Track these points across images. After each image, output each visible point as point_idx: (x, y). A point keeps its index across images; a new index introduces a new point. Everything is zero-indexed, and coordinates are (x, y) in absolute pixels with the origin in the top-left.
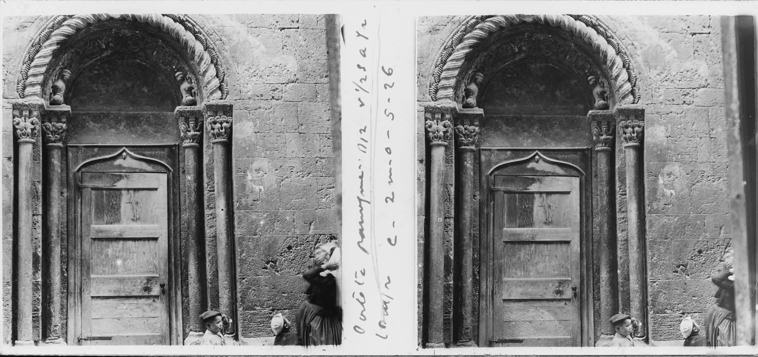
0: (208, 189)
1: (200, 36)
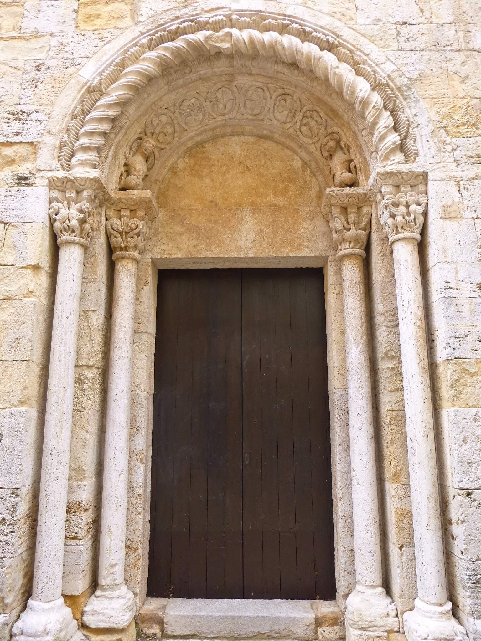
0: (386, 323)
1: (364, 66)
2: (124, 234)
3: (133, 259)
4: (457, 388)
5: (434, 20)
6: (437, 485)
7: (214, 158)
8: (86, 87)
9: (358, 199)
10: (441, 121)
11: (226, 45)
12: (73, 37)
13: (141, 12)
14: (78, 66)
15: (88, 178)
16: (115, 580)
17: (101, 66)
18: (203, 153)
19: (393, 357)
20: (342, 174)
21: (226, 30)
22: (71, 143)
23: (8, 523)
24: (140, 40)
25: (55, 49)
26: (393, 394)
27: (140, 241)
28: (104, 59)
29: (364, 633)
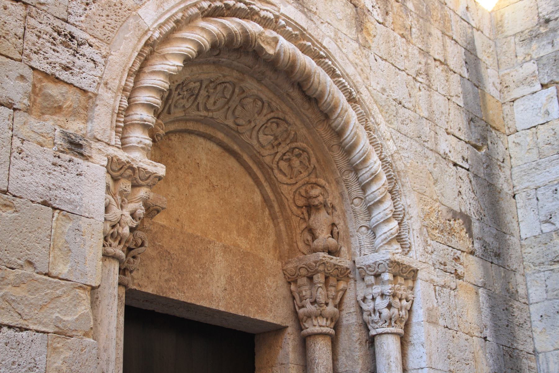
7: (181, 159)
8: (146, 38)
15: (154, 173)
18: (169, 147)
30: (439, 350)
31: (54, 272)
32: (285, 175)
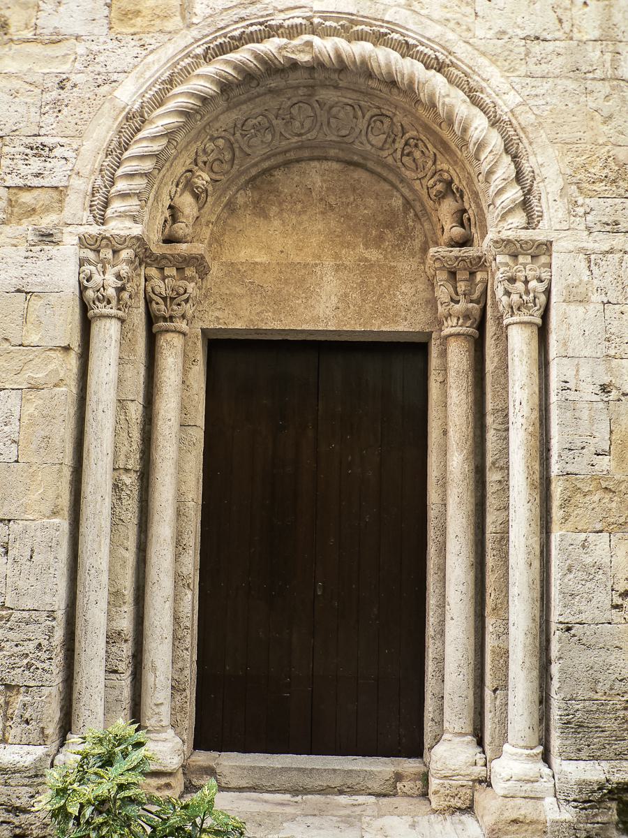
0: (494, 426)
1: (481, 95)
2: (168, 299)
3: (179, 332)
4: (566, 509)
5: (576, 35)
6: (538, 619)
8: (124, 113)
9: (471, 262)
10: (573, 175)
11: (304, 58)
12: (105, 42)
13: (194, 10)
14: (114, 84)
16: (161, 720)
17: (144, 83)
18: (270, 183)
19: (502, 468)
20: (451, 228)
21: (306, 37)
22: (105, 187)
23: (45, 649)
24: (194, 50)
25: (83, 59)
26: (498, 512)
27: (189, 309)
28: (148, 75)
29: (446, 782)
30: (587, 333)
31: (26, 343)
32: (412, 170)
